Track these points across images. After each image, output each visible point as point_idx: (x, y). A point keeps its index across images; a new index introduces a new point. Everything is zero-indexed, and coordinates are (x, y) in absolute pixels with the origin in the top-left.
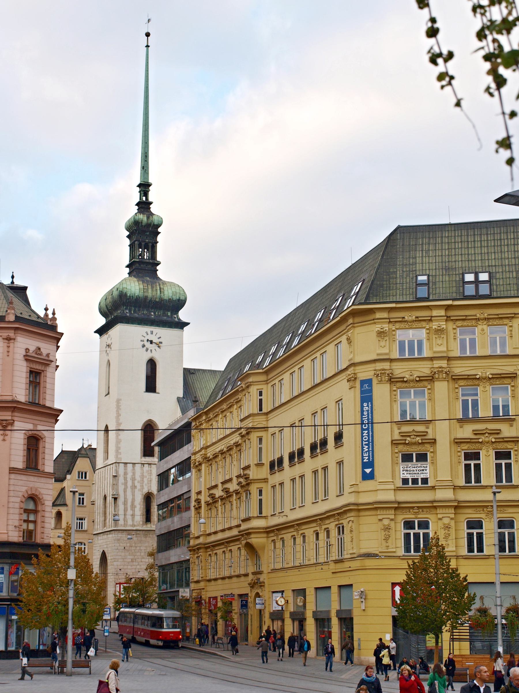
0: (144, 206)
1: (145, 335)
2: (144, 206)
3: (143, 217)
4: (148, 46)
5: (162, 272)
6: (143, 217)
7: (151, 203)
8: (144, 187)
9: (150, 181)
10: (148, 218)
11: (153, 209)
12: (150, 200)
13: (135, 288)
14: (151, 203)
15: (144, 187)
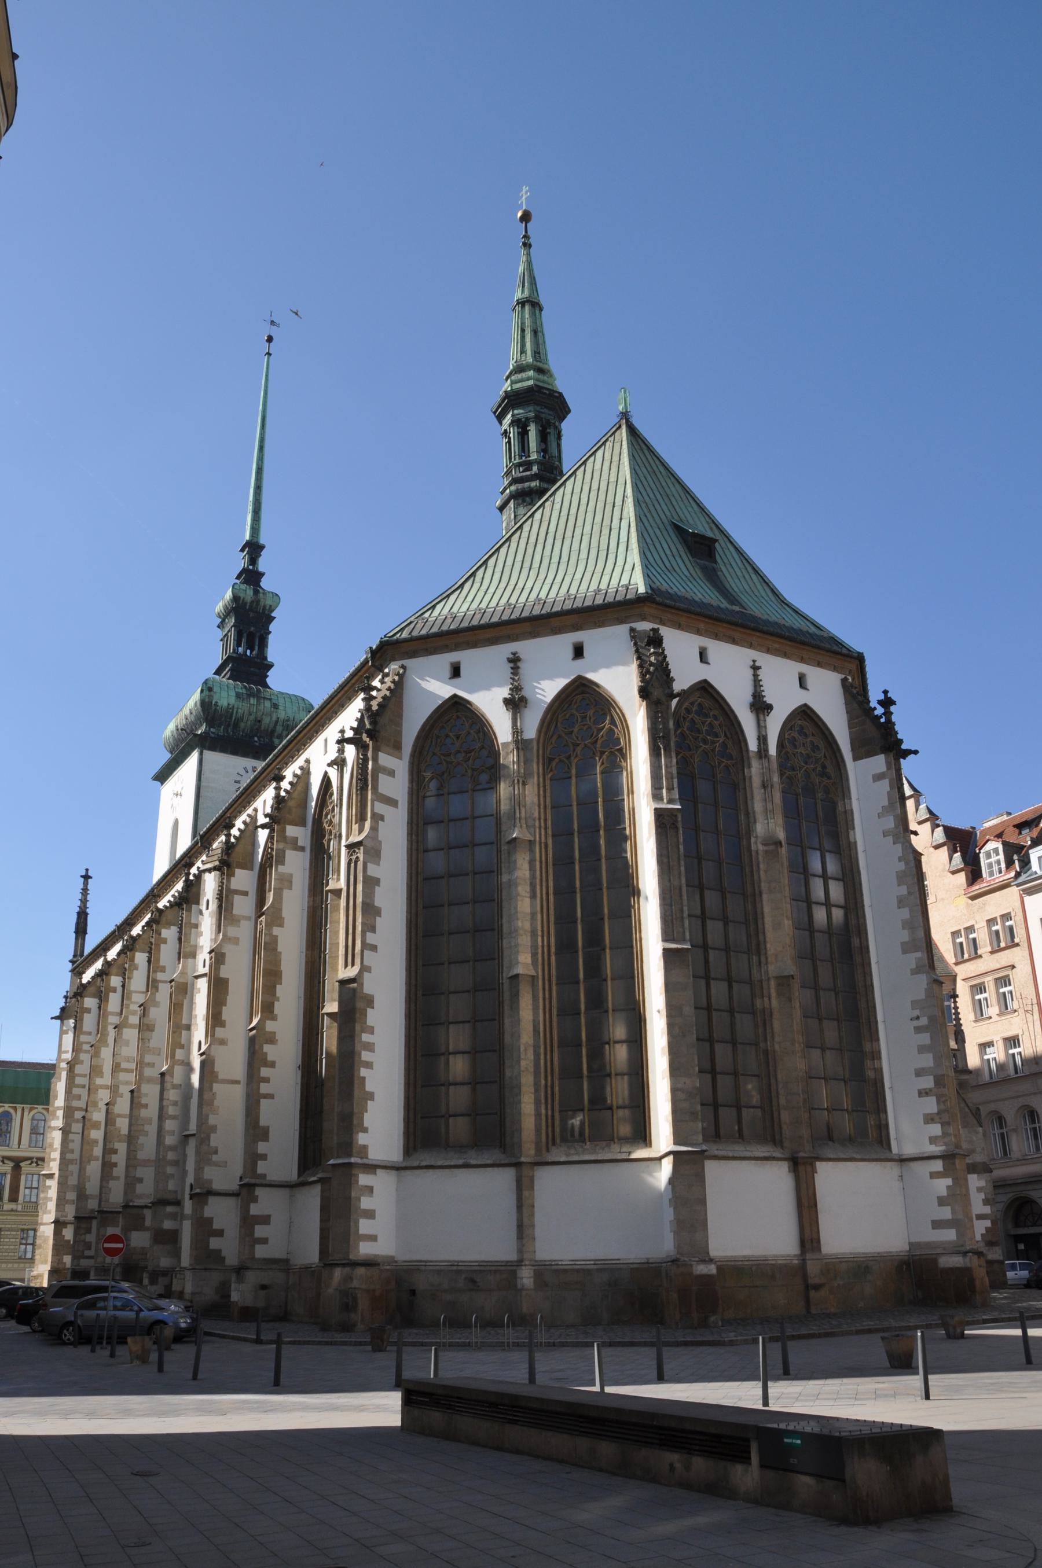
0: (251, 576)
1: (243, 772)
2: (251, 576)
3: (248, 593)
4: (269, 354)
5: (275, 680)
6: (248, 593)
7: (262, 574)
8: (254, 549)
9: (262, 541)
10: (256, 592)
11: (265, 583)
12: (261, 569)
13: (227, 696)
14: (262, 574)
15: (254, 549)
